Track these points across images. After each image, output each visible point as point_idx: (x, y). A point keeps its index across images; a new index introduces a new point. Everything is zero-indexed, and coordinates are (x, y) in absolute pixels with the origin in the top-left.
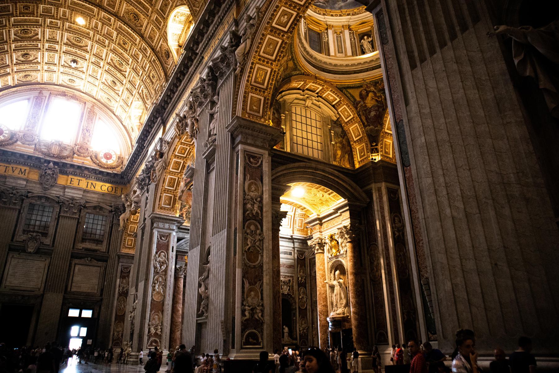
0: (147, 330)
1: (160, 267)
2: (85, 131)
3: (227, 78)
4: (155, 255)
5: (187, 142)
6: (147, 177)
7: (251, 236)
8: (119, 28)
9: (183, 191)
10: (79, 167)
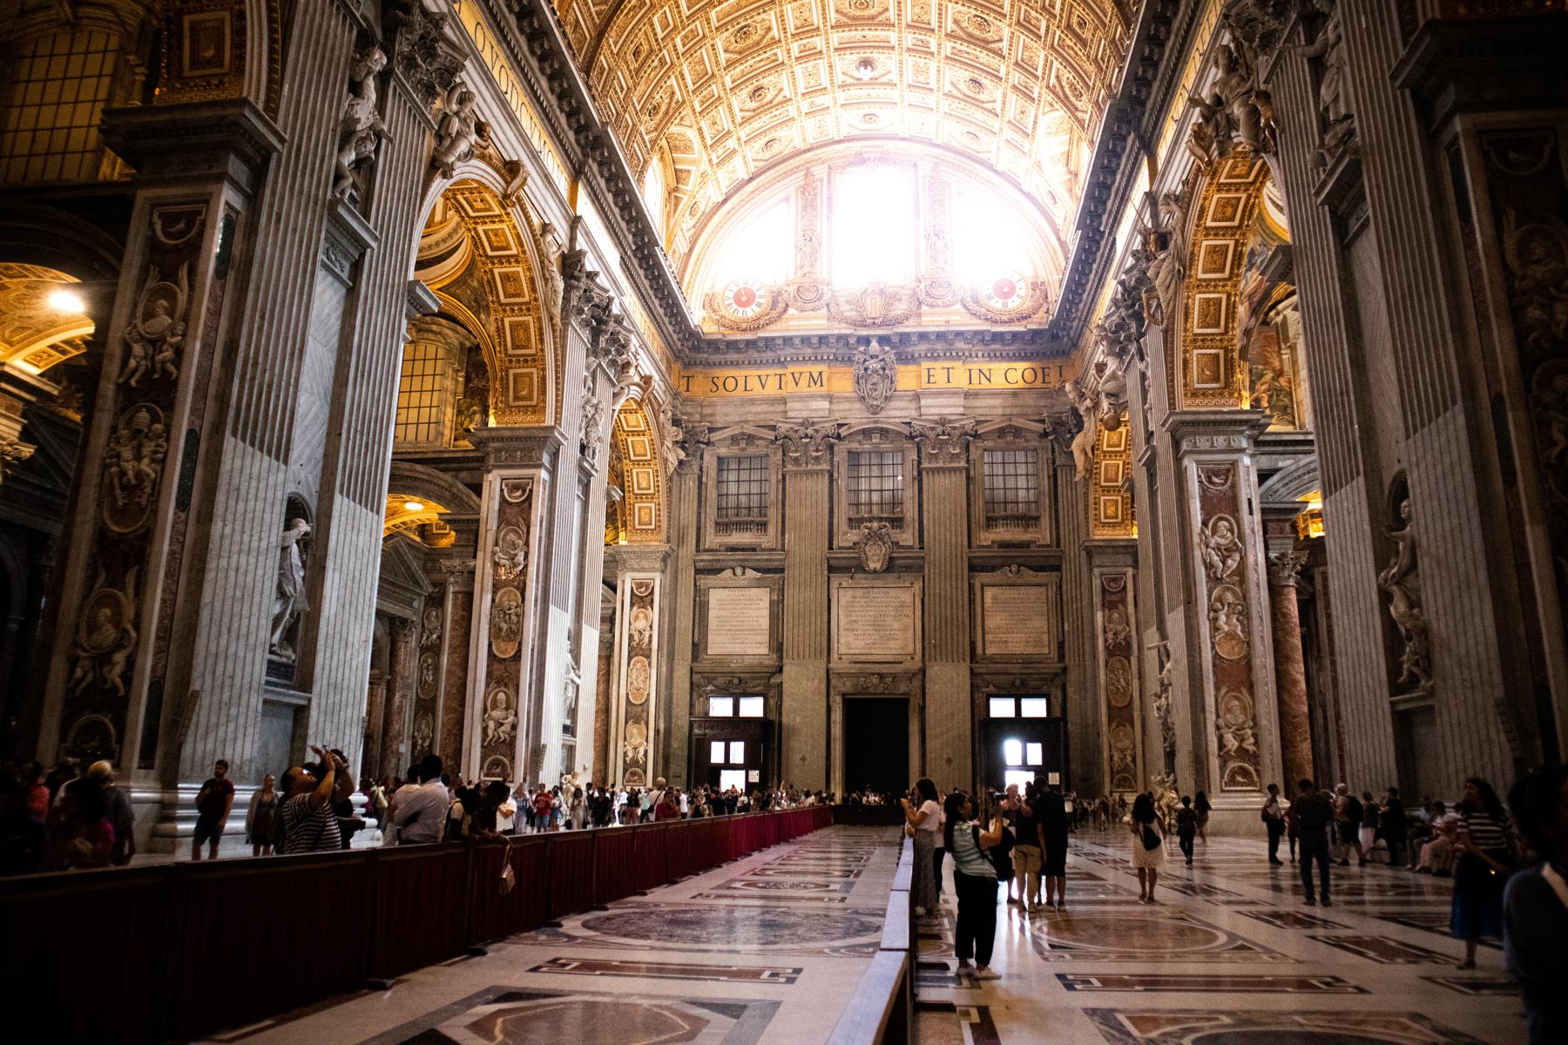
0: (1215, 740)
1: (1224, 563)
2: (932, 236)
4: (1203, 532)
5: (1238, 177)
6: (1130, 316)
9: (1247, 333)
10: (940, 336)
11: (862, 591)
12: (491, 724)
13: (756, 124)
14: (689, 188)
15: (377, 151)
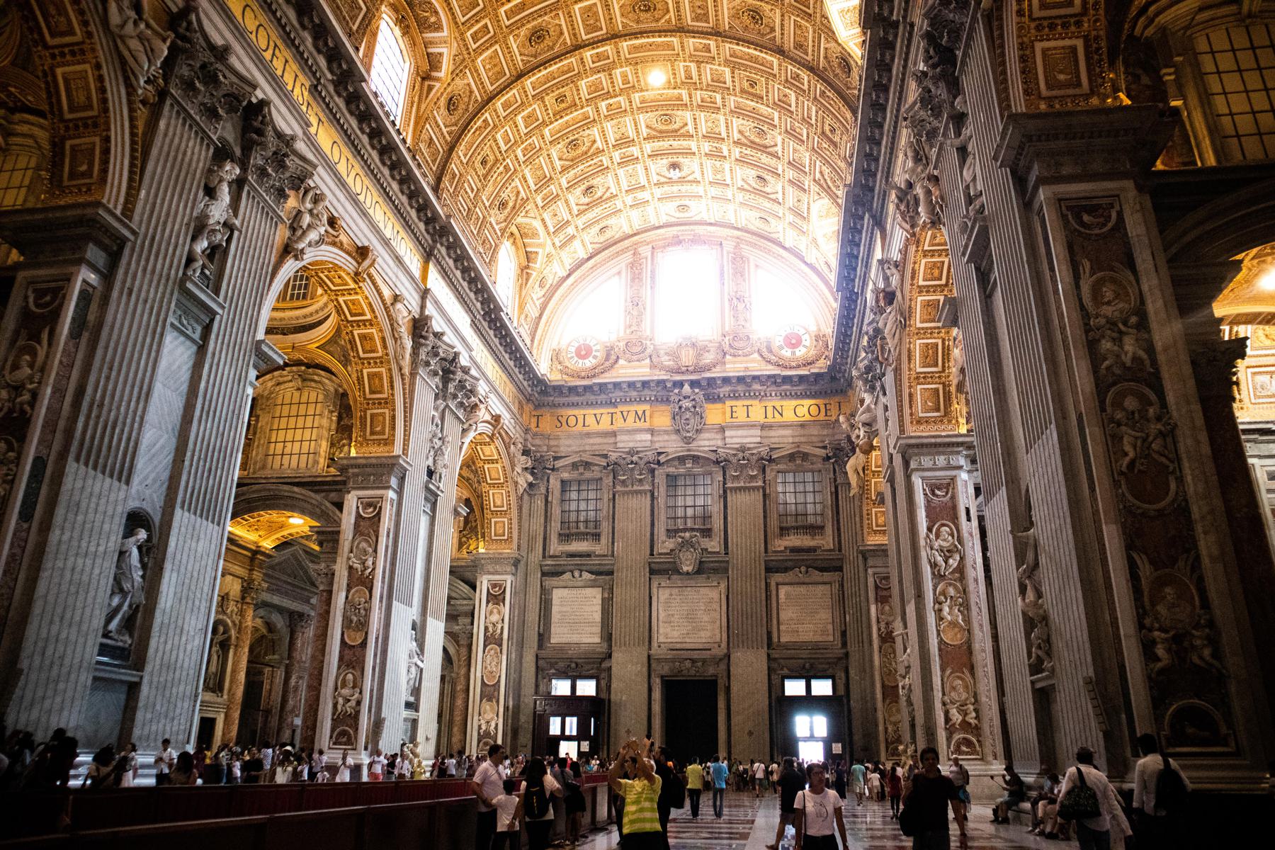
1: (946, 563)
2: (735, 300)
3: (970, 37)
4: (928, 536)
7: (1133, 428)
8: (731, 56)
10: (741, 380)
11: (677, 590)
12: (341, 701)
13: (590, 215)
14: (537, 266)
15: (229, 241)
